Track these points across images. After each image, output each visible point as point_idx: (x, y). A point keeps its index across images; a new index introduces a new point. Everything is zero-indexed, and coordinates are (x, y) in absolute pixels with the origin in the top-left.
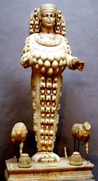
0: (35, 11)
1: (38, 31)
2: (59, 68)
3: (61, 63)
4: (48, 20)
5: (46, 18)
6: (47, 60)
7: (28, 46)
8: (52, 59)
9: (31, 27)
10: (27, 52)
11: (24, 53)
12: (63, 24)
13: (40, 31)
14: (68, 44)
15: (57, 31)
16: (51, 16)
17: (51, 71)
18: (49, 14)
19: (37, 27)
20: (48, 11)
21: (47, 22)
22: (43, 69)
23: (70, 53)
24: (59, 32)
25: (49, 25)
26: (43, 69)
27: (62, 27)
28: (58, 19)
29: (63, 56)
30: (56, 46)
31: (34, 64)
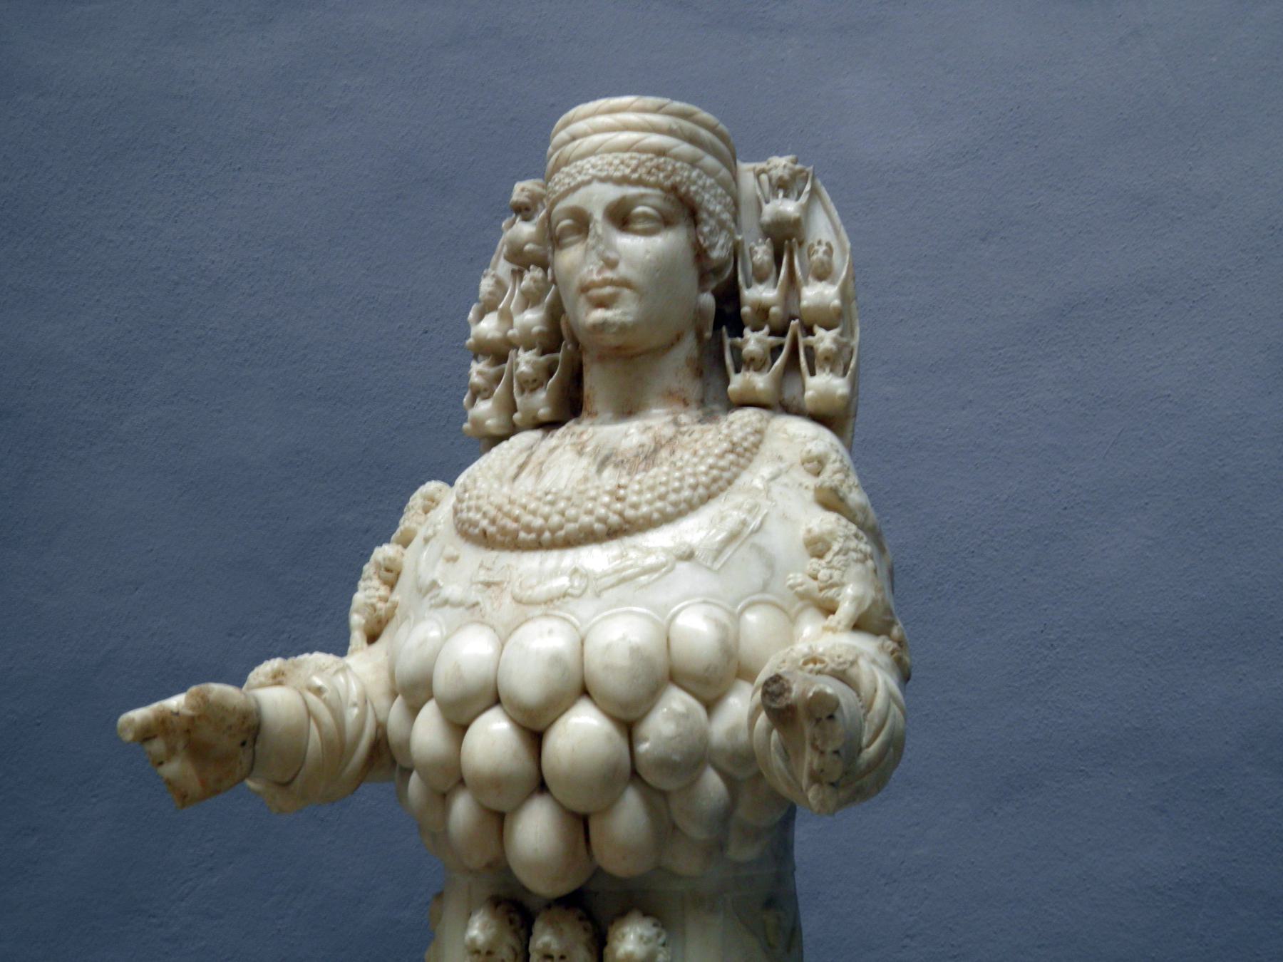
0: (524, 211)
1: (541, 402)
2: (655, 798)
3: (671, 716)
4: (592, 272)
5: (570, 257)
6: (497, 701)
7: (391, 576)
8: (527, 681)
9: (478, 371)
10: (372, 638)
11: (339, 647)
12: (817, 294)
13: (571, 406)
14: (831, 501)
15: (737, 382)
16: (621, 217)
17: (535, 830)
18: (598, 197)
19: (525, 361)
20: (589, 166)
21: (585, 289)
22: (462, 809)
23: (846, 609)
24: (760, 381)
25: (599, 315)
26: (462, 809)
27: (809, 331)
28: (761, 253)
29: (696, 629)
30: (613, 533)
31: (385, 755)
